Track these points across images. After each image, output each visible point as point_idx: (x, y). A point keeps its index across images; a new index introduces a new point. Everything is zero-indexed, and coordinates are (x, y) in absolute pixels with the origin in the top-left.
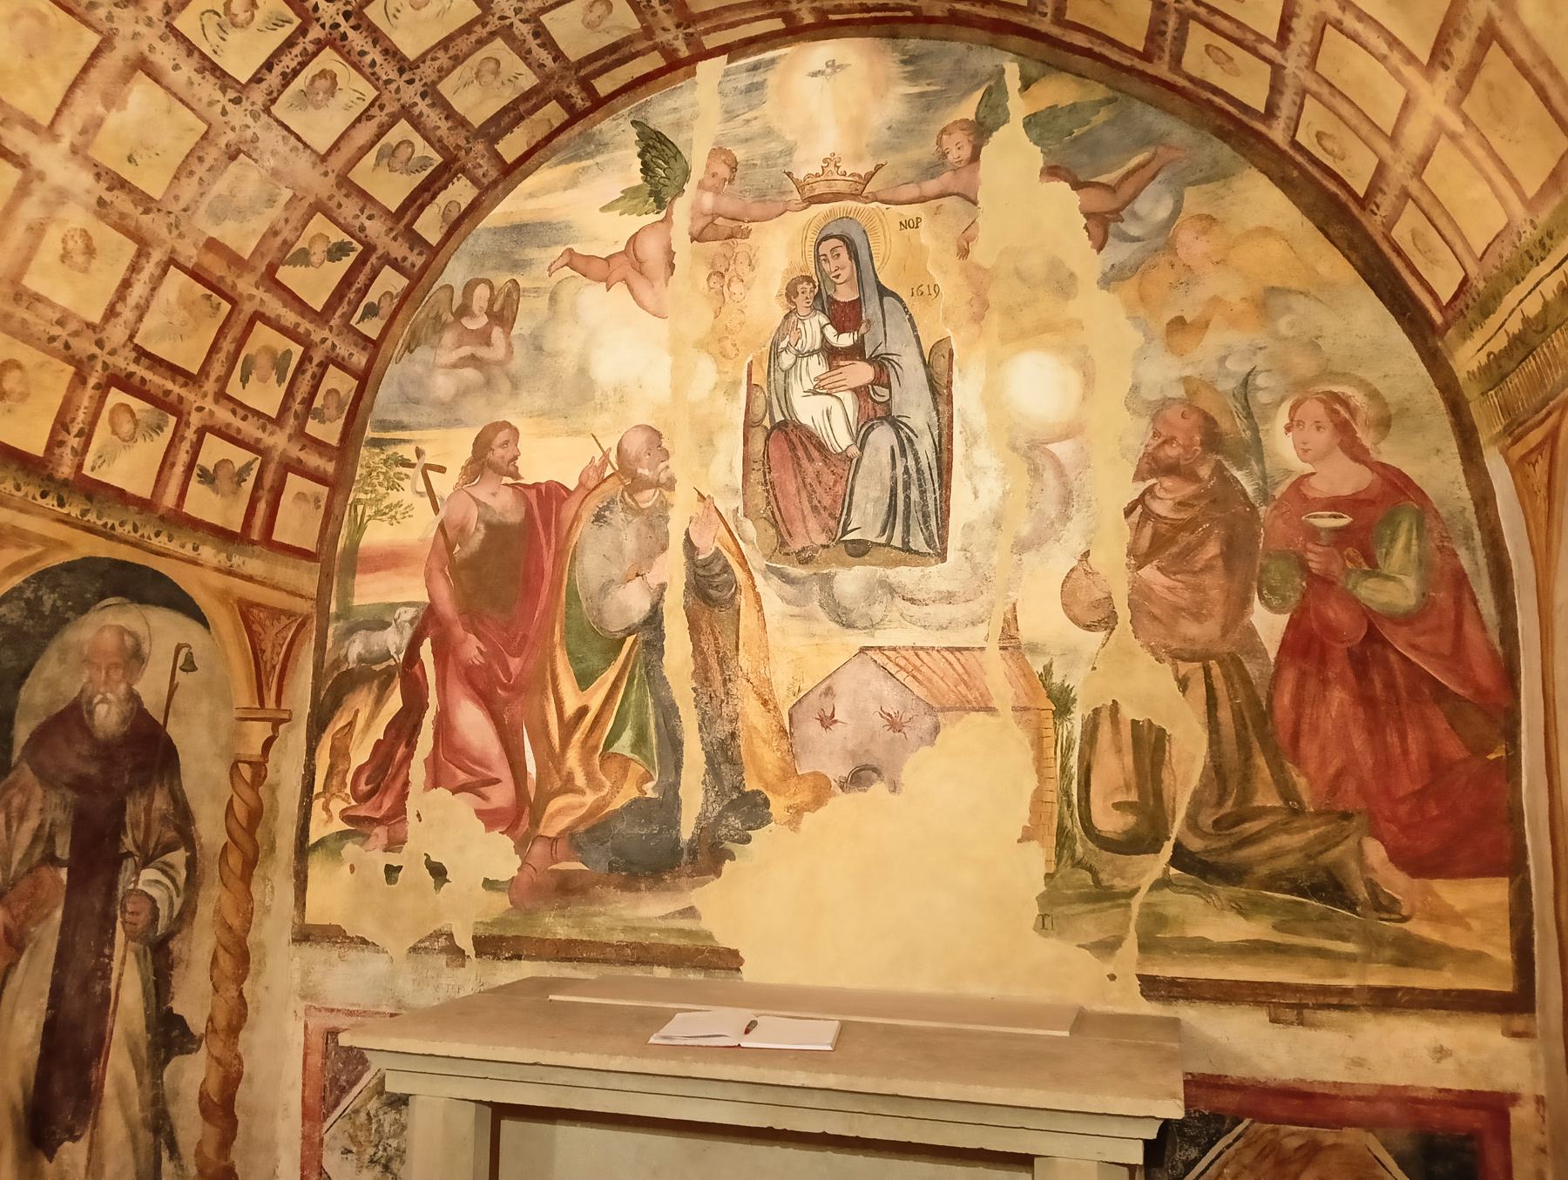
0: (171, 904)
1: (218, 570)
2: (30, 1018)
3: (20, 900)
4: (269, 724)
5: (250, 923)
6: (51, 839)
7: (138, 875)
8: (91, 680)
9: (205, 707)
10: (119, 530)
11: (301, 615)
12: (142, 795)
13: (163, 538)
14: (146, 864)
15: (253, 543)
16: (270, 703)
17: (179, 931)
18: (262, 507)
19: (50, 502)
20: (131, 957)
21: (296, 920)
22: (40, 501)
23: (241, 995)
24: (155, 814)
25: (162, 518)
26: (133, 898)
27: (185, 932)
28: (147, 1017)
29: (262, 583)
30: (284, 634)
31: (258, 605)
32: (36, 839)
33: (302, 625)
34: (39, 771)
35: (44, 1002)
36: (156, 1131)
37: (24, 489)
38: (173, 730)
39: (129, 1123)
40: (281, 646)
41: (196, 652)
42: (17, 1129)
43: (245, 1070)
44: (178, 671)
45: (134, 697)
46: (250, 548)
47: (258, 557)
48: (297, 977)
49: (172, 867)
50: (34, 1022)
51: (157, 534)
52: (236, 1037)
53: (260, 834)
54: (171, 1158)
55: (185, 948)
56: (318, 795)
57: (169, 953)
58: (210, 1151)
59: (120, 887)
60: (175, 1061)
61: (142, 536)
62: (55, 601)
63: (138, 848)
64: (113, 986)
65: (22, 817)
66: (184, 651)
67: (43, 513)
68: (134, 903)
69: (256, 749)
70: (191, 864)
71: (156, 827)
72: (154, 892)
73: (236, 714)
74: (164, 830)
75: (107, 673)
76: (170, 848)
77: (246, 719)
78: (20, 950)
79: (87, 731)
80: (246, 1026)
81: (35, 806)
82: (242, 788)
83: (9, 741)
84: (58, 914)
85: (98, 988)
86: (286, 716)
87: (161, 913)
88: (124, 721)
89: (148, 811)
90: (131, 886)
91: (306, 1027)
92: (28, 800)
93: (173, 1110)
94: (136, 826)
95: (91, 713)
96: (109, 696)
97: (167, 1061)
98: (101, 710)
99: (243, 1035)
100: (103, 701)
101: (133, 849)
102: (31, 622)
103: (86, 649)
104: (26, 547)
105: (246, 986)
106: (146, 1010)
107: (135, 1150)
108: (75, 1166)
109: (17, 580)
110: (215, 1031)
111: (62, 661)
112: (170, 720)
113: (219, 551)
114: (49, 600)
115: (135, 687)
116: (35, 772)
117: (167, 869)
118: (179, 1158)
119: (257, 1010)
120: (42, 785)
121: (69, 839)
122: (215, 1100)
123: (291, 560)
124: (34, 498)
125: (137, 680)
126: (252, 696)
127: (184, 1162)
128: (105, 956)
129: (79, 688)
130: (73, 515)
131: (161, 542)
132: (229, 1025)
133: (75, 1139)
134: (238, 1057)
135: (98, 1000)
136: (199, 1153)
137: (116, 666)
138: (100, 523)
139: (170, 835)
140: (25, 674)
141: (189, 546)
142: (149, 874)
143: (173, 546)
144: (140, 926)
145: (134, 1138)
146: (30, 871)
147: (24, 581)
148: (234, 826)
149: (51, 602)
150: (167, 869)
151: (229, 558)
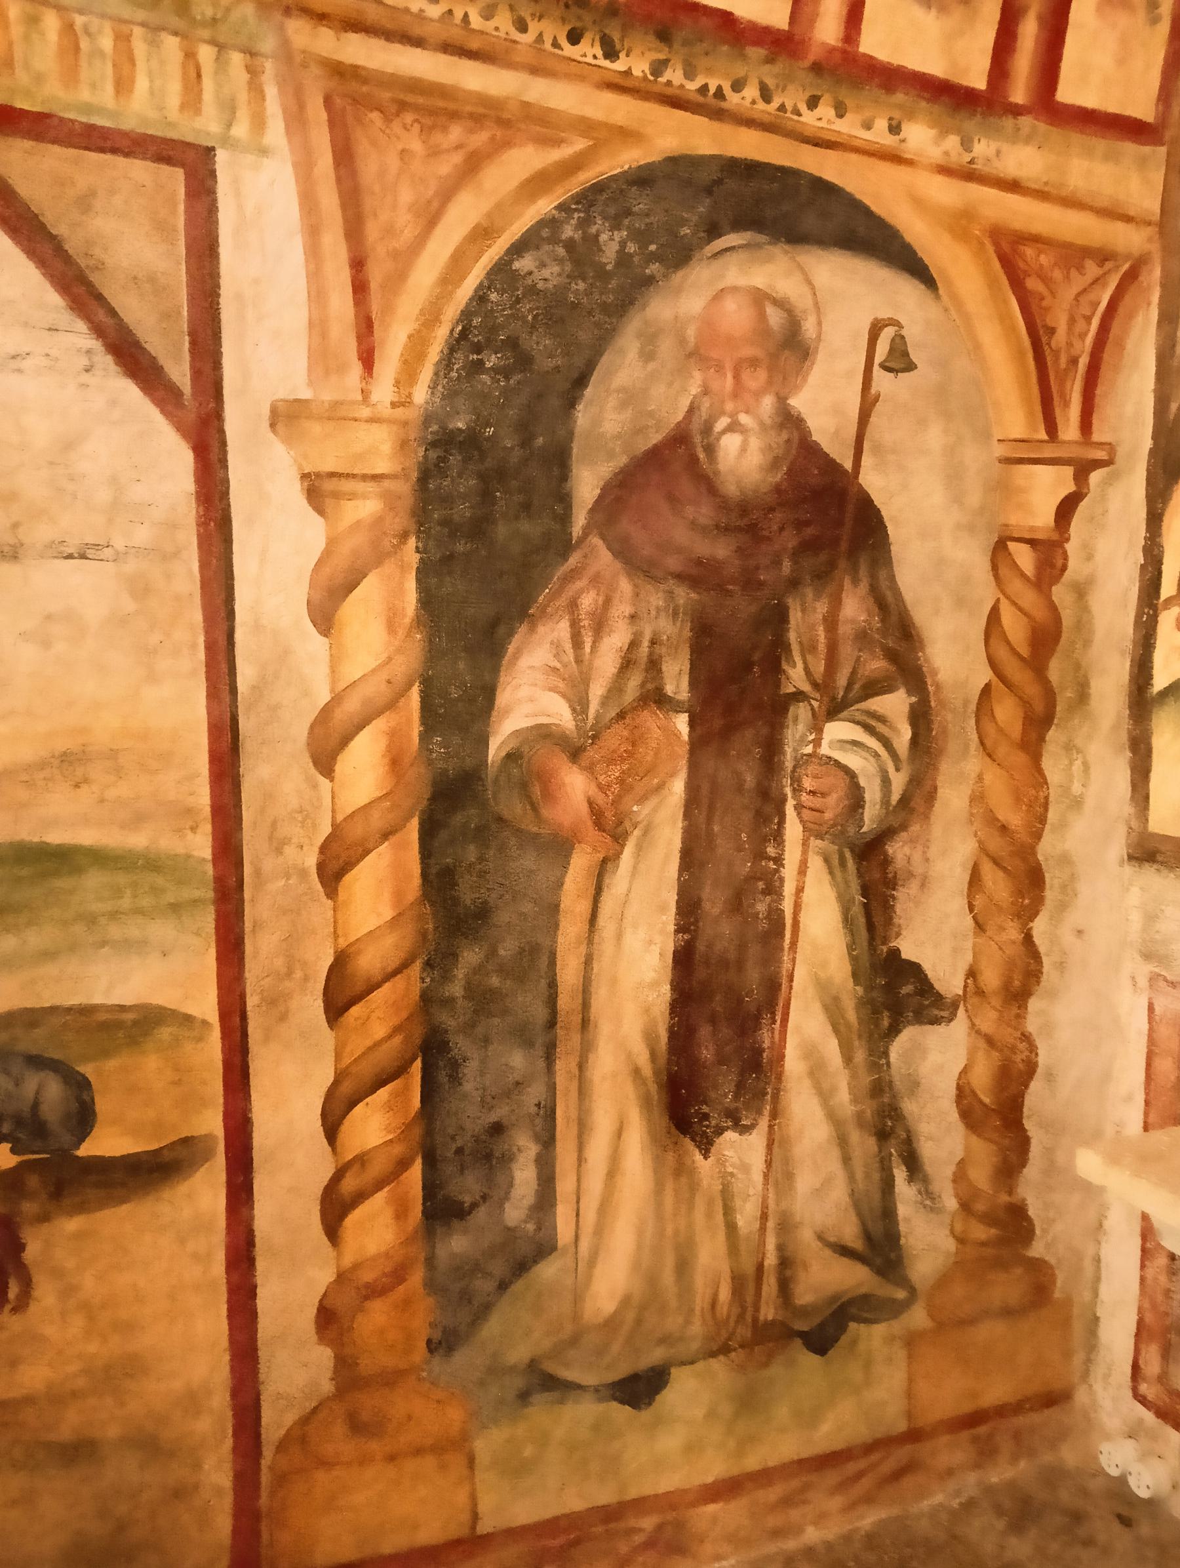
0: (886, 782)
1: (945, 170)
2: (650, 942)
3: (611, 761)
4: (1069, 471)
5: (1043, 820)
6: (654, 665)
7: (819, 731)
8: (706, 391)
9: (935, 437)
10: (733, 99)
11: (1128, 257)
12: (818, 597)
13: (825, 111)
14: (834, 711)
15: (1016, 111)
16: (1070, 430)
17: (904, 827)
18: (1029, 31)
19: (589, 50)
20: (816, 864)
21: (1134, 824)
22: (569, 50)
23: (1028, 939)
24: (845, 630)
25: (817, 68)
26: (811, 769)
27: (915, 828)
28: (854, 960)
29: (1041, 195)
30: (1092, 296)
31: (1035, 239)
32: (627, 664)
33: (1131, 276)
34: (624, 552)
35: (669, 919)
36: (883, 1135)
37: (534, 27)
38: (872, 480)
39: (832, 1116)
40: (1088, 319)
41: (913, 333)
42: (646, 1103)
43: (1042, 1059)
44: (876, 368)
45: (790, 421)
46: (1008, 122)
47: (1028, 140)
48: (1136, 919)
49: (882, 719)
50: (656, 949)
51: (813, 103)
52: (1023, 1006)
53: (1055, 670)
54: (911, 1179)
55: (917, 857)
56: (1169, 602)
57: (886, 862)
58: (981, 1176)
59: (789, 750)
60: (908, 1034)
61: (782, 108)
62: (623, 244)
63: (815, 685)
64: (787, 906)
65: (600, 626)
66: (888, 334)
67: (576, 73)
68: (816, 777)
69: (1043, 517)
70: (920, 717)
71: (847, 652)
72: (852, 760)
73: (1000, 451)
74: (864, 656)
75: (737, 377)
76: (874, 688)
77: (1021, 461)
78: (619, 839)
79: (707, 483)
80: (1040, 990)
81: (622, 609)
82: (1016, 586)
83: (564, 499)
84: (678, 787)
85: (761, 907)
86: (1101, 455)
87: (867, 796)
88: (775, 464)
89: (831, 622)
90: (809, 749)
91: (1151, 1008)
92: (608, 602)
93: (909, 1107)
94: (809, 648)
95: (710, 450)
96: (744, 419)
97: (894, 1030)
98: (730, 444)
99: (1034, 1004)
100: (733, 427)
101: (806, 687)
102: (581, 286)
103: (691, 333)
104: (557, 142)
105: (1039, 927)
106: (850, 947)
107: (846, 1160)
108: (746, 1168)
109: (545, 206)
110: (980, 993)
111: (648, 356)
112: (867, 461)
113: (944, 132)
114: (611, 243)
115: (793, 402)
116: (617, 554)
117: (872, 724)
118: (926, 1180)
119: (1061, 966)
120: (630, 575)
121: (686, 667)
122: (987, 1100)
123: (1101, 145)
124: (556, 44)
125: (797, 388)
126: (1030, 414)
127: (935, 1187)
128: (769, 858)
129: (684, 404)
130: (637, 72)
131: (821, 119)
132: (1007, 986)
133: (745, 1130)
134: (1026, 1038)
135: (764, 925)
136: (960, 1175)
137: (754, 363)
138: (692, 86)
139: (876, 665)
140: (581, 381)
141: (881, 124)
142: (837, 730)
143: (847, 127)
144: (828, 815)
145: (842, 1141)
146: (621, 716)
147: (560, 207)
148: (1002, 653)
149: (615, 246)
150: (873, 723)
151: (966, 144)
